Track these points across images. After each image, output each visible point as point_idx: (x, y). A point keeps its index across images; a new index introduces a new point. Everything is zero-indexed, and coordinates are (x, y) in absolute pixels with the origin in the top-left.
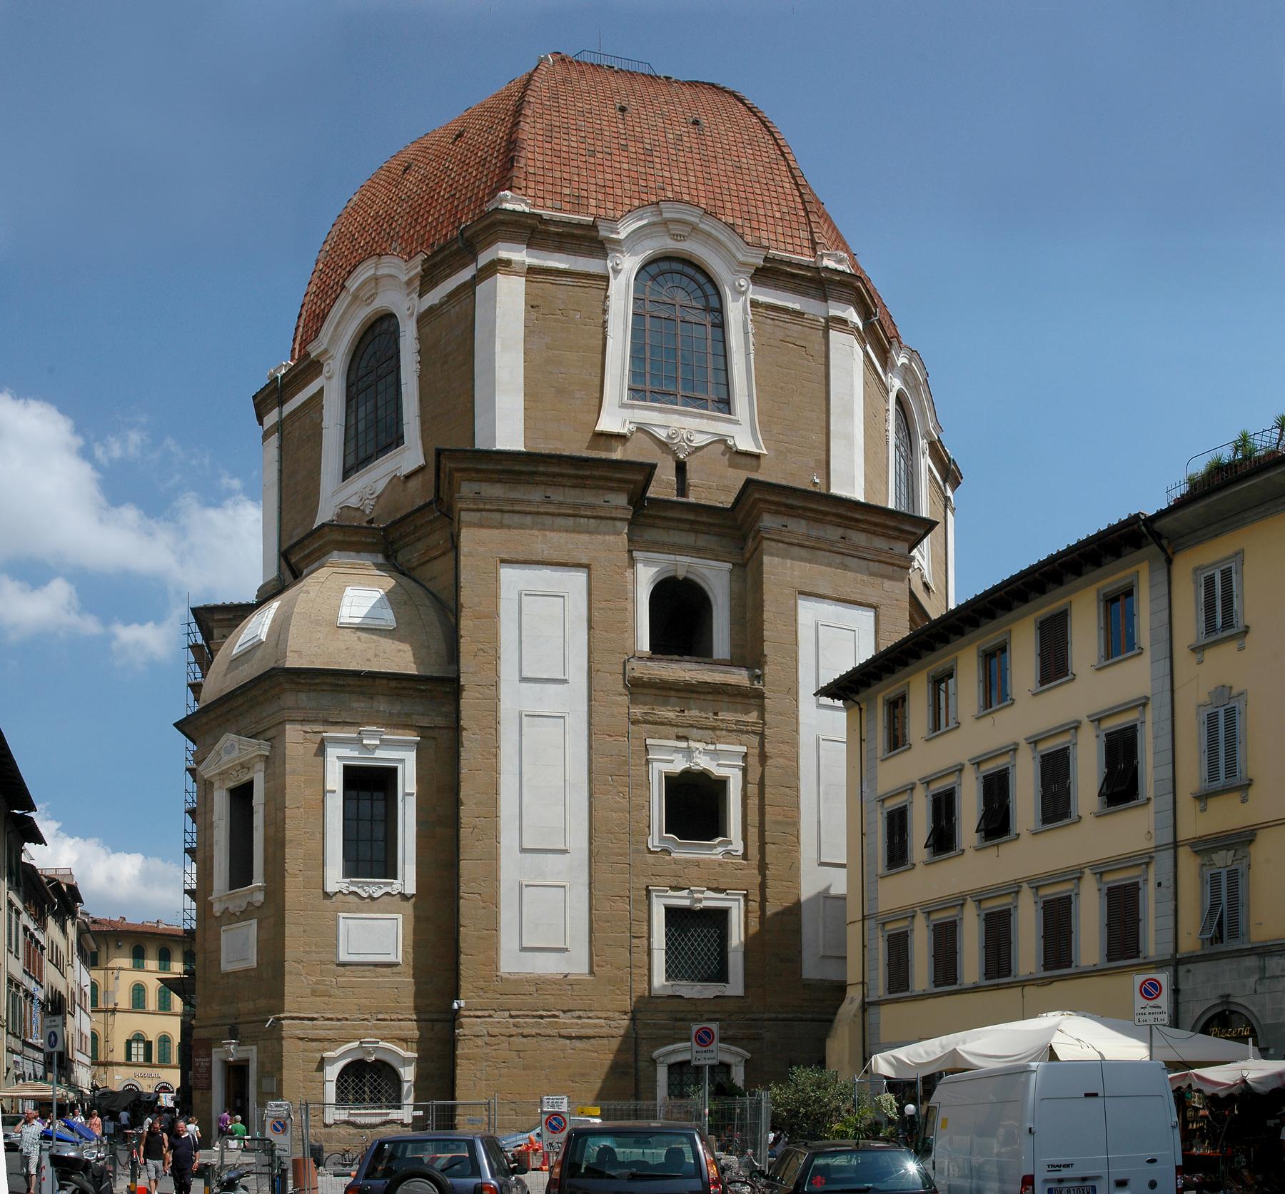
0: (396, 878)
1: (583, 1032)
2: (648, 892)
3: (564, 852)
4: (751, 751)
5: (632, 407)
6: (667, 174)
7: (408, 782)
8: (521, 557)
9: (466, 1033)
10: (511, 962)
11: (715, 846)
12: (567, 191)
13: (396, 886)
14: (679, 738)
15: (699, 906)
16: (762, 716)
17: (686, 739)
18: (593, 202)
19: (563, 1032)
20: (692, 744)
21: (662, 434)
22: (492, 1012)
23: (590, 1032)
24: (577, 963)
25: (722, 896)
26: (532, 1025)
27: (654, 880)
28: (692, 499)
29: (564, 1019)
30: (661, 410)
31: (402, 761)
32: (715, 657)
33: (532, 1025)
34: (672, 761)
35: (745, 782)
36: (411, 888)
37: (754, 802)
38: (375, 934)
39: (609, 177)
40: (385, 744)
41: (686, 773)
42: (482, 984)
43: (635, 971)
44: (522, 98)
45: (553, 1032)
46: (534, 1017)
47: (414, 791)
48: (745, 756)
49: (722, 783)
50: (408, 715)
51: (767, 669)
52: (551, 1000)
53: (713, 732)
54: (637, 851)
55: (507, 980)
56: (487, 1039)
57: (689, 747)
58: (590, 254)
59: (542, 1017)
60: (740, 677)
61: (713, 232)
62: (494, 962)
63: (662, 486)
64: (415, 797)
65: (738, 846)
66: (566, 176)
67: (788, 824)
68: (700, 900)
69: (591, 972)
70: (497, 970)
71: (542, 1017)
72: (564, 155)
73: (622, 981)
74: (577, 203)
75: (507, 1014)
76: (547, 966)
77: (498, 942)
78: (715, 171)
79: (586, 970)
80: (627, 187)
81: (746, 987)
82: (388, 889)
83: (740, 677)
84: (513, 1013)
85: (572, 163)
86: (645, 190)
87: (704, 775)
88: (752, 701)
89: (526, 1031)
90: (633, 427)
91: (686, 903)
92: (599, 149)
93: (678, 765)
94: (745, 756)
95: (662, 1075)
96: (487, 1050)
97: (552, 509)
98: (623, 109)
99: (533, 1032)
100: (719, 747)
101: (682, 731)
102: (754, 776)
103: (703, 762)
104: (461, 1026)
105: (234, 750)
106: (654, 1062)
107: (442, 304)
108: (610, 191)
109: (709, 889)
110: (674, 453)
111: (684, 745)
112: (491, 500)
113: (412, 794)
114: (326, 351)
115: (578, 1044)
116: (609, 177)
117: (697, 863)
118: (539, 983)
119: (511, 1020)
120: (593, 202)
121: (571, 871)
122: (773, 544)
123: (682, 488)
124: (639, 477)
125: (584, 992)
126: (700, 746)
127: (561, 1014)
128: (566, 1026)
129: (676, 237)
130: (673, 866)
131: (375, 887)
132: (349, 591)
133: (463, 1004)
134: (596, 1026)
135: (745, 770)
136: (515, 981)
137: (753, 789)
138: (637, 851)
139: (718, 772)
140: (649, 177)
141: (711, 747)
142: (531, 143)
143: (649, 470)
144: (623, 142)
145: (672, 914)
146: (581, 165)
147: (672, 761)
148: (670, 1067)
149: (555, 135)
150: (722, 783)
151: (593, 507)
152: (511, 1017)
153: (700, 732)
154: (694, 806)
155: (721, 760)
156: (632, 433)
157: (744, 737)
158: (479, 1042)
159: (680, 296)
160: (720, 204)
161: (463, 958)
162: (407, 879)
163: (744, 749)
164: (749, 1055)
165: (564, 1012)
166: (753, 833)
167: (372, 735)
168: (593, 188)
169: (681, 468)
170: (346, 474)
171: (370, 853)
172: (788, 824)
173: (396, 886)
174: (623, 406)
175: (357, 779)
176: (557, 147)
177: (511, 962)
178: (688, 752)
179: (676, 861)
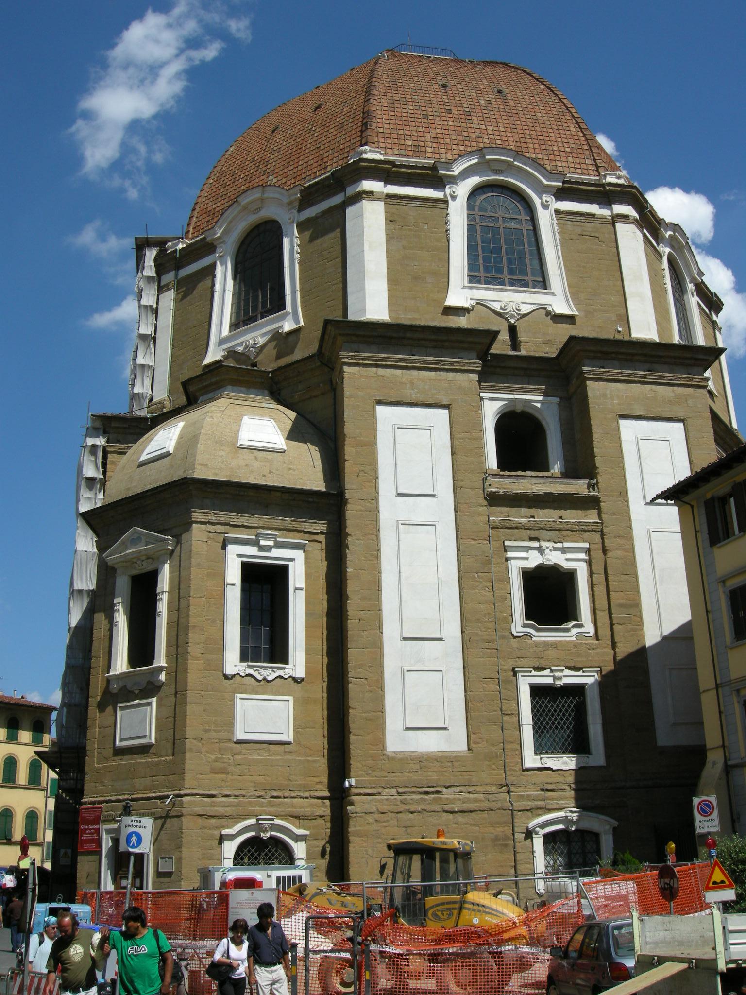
0: (287, 663)
1: (466, 806)
2: (515, 674)
3: (440, 639)
4: (593, 546)
5: (471, 288)
6: (483, 127)
7: (297, 578)
8: (389, 399)
9: (358, 810)
10: (397, 741)
11: (568, 630)
12: (409, 143)
13: (288, 671)
14: (532, 539)
15: (559, 683)
16: (600, 517)
17: (538, 539)
18: (429, 150)
19: (446, 807)
20: (544, 544)
21: (497, 307)
22: (380, 790)
23: (471, 806)
24: (455, 740)
25: (580, 673)
26: (418, 802)
27: (520, 662)
28: (523, 352)
29: (446, 793)
30: (494, 289)
31: (292, 560)
33: (418, 802)
34: (527, 559)
35: (591, 573)
37: (601, 590)
38: (268, 715)
39: (439, 131)
40: (279, 545)
41: (540, 568)
42: (370, 762)
43: (507, 746)
44: (370, 82)
45: (438, 807)
46: (420, 793)
47: (303, 586)
48: (588, 551)
49: (571, 576)
51: (600, 479)
52: (434, 776)
53: (559, 532)
54: (503, 637)
55: (393, 759)
56: (377, 816)
57: (540, 547)
59: (426, 793)
60: (579, 487)
62: (381, 741)
64: (303, 592)
65: (589, 628)
66: (407, 132)
67: (631, 606)
68: (560, 678)
69: (469, 749)
70: (384, 749)
71: (426, 793)
72: (404, 119)
73: (497, 756)
74: (418, 151)
75: (394, 791)
76: (429, 744)
77: (384, 723)
78: (519, 123)
79: (466, 748)
80: (454, 137)
81: (608, 757)
82: (280, 673)
83: (579, 487)
84: (400, 790)
85: (411, 124)
86: (467, 139)
89: (413, 808)
90: (474, 303)
91: (550, 681)
92: (430, 113)
93: (533, 560)
94: (588, 551)
95: (538, 843)
96: (376, 827)
98: (444, 86)
99: (419, 808)
100: (566, 545)
101: (534, 533)
102: (598, 568)
103: (555, 558)
104: (352, 804)
105: (136, 543)
106: (529, 834)
108: (442, 141)
109: (568, 668)
110: (506, 319)
111: (536, 544)
113: (301, 589)
114: (219, 238)
115: (460, 818)
116: (439, 131)
117: (554, 645)
118: (423, 761)
119: (398, 797)
120: (429, 150)
121: (448, 654)
123: (515, 343)
125: (463, 769)
126: (550, 545)
127: (444, 790)
128: (449, 801)
129: (496, 172)
130: (535, 649)
131: (268, 671)
132: (245, 419)
133: (353, 782)
134: (476, 800)
135: (589, 563)
136: (401, 760)
137: (599, 578)
138: (503, 637)
139: (567, 565)
140: (470, 130)
141: (559, 545)
142: (379, 112)
144: (447, 108)
145: (537, 691)
146: (418, 124)
147: (527, 559)
148: (545, 836)
149: (396, 106)
150: (571, 576)
152: (399, 794)
153: (549, 533)
154: (549, 595)
155: (568, 557)
156: (473, 307)
157: (586, 535)
158: (370, 819)
159: (506, 205)
160: (525, 145)
161: (352, 737)
163: (587, 545)
164: (615, 823)
165: (447, 788)
166: (603, 617)
167: (267, 537)
168: (429, 139)
169: (512, 330)
172: (631, 606)
173: (288, 671)
174: (465, 287)
176: (399, 114)
177: (397, 741)
178: (541, 550)
179: (537, 644)
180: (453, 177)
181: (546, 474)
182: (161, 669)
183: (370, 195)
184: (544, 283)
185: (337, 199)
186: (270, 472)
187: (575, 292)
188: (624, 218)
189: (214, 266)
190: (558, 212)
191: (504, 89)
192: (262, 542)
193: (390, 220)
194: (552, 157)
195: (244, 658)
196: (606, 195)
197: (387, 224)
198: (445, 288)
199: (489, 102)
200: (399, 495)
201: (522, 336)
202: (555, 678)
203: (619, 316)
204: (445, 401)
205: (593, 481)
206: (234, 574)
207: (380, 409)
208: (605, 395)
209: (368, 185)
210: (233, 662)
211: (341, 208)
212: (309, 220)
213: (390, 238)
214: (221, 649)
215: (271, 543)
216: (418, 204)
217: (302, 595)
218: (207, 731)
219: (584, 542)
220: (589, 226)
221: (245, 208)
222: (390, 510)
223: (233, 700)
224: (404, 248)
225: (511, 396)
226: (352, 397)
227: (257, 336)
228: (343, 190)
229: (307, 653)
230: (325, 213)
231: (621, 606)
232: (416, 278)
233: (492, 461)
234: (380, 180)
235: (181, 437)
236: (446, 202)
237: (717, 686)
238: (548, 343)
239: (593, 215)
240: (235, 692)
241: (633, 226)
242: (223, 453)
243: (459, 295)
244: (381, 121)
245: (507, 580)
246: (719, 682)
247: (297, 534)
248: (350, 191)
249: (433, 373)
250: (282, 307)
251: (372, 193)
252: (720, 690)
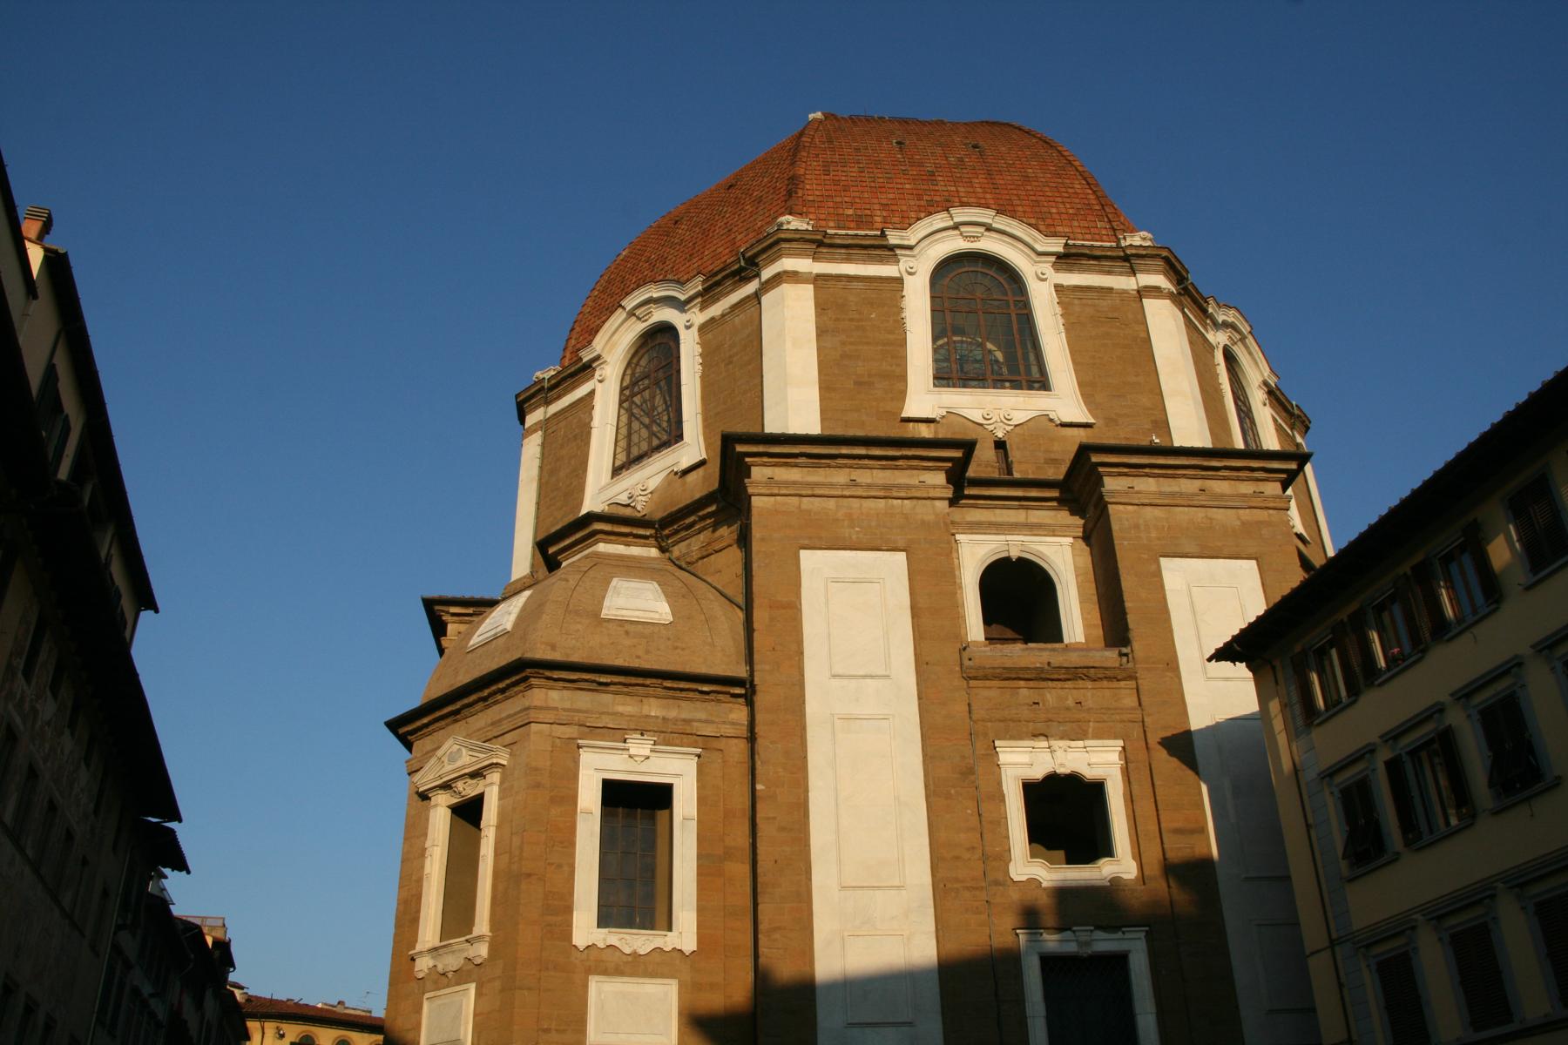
7: (685, 804)
12: (850, 212)
14: (1035, 736)
20: (1053, 742)
25: (1119, 935)
31: (678, 775)
32: (1066, 640)
36: (689, 943)
37: (1145, 807)
41: (1052, 779)
50: (687, 721)
51: (1136, 645)
58: (881, 260)
61: (1008, 229)
63: (984, 463)
67: (1192, 832)
68: (1088, 944)
87: (1074, 779)
88: (1122, 683)
97: (860, 492)
101: (1041, 727)
107: (723, 316)
109: (1098, 928)
112: (787, 484)
122: (1121, 507)
124: (958, 454)
132: (615, 581)
139: (1089, 773)
143: (968, 447)
151: (908, 487)
162: (684, 933)
170: (617, 471)
171: (634, 893)
172: (1192, 832)
173: (668, 941)
175: (618, 795)
180: (910, 248)
181: (1057, 645)
182: (480, 938)
183: (794, 277)
184: (1042, 383)
185: (751, 288)
186: (647, 652)
187: (1088, 389)
188: (1155, 291)
189: (592, 392)
190: (1059, 288)
191: (981, 143)
192: (632, 751)
193: (821, 308)
194: (1049, 221)
195: (604, 920)
196: (1129, 261)
197: (818, 315)
198: (902, 395)
199: (961, 160)
200: (834, 676)
201: (1014, 455)
202: (1080, 944)
203: (1155, 422)
204: (901, 544)
205: (1124, 650)
206: (589, 798)
207: (803, 553)
208: (1137, 526)
209: (788, 264)
210: (585, 929)
211: (757, 297)
212: (713, 319)
213: (821, 332)
214: (568, 910)
215: (647, 753)
216: (860, 285)
217: (694, 825)
218: (547, 1031)
219: (1116, 738)
220: (1104, 304)
221: (631, 314)
222: (823, 697)
223: (585, 986)
224: (843, 343)
225: (1002, 537)
226: (763, 540)
227: (651, 477)
228: (758, 275)
229: (701, 911)
230: (734, 307)
231: (1178, 831)
232: (858, 383)
233: (975, 628)
234: (807, 256)
235: (523, 609)
236: (899, 281)
237: (1332, 943)
238: (1054, 462)
239: (1110, 290)
240: (590, 971)
241: (1168, 302)
242: (579, 627)
243: (925, 400)
244: (812, 188)
245: (1001, 798)
246: (1334, 936)
247: (685, 739)
248: (767, 274)
249: (881, 503)
250: (680, 437)
251: (795, 273)
252: (1337, 949)
